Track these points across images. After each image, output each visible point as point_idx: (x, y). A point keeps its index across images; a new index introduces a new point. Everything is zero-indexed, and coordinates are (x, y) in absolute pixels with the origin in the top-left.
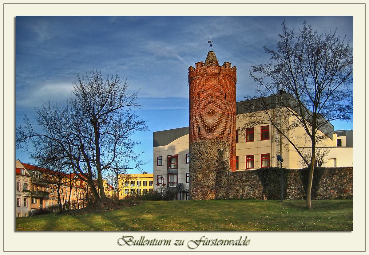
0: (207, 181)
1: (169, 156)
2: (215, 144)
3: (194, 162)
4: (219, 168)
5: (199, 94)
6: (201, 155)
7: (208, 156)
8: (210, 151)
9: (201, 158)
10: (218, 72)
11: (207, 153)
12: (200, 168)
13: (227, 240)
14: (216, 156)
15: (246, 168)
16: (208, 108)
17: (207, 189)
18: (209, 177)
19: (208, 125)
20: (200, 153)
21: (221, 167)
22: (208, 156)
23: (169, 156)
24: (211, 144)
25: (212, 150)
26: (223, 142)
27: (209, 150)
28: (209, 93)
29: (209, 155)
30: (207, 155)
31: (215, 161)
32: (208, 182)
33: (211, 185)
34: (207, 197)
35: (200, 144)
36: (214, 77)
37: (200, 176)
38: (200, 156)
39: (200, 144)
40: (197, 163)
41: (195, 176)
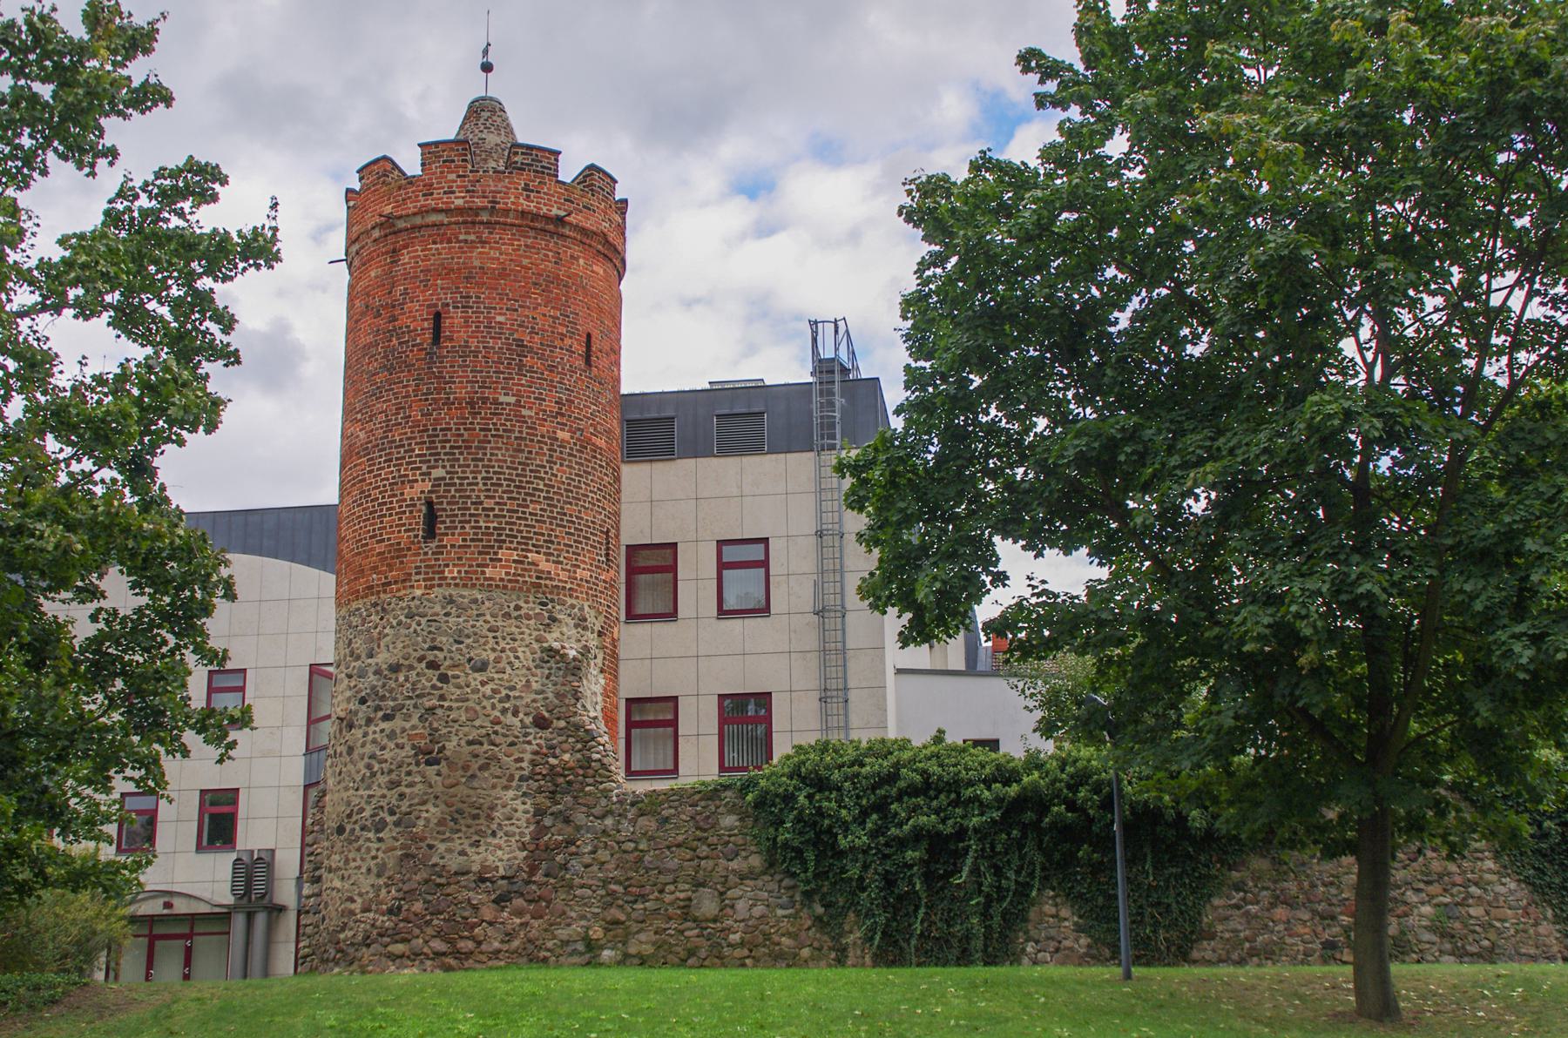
0: (476, 844)
1: (205, 842)
2: (528, 617)
3: (387, 718)
4: (552, 761)
5: (438, 317)
6: (444, 678)
7: (487, 689)
8: (497, 660)
9: (442, 698)
10: (555, 211)
11: (482, 667)
12: (428, 763)
13: (191, 694)
14: (535, 686)
15: (722, 768)
16: (496, 402)
17: (477, 898)
18: (490, 818)
19: (488, 503)
20: (433, 665)
21: (566, 757)
22: (487, 689)
23: (205, 842)
24: (507, 615)
25: (514, 650)
26: (573, 606)
27: (494, 650)
28: (500, 319)
29: (492, 680)
30: (483, 683)
31: (528, 720)
32: (482, 849)
33: (502, 872)
34: (470, 945)
35: (438, 608)
36: (532, 234)
37: (433, 810)
38: (434, 687)
39: (438, 608)
40: (407, 725)
41: (392, 813)
